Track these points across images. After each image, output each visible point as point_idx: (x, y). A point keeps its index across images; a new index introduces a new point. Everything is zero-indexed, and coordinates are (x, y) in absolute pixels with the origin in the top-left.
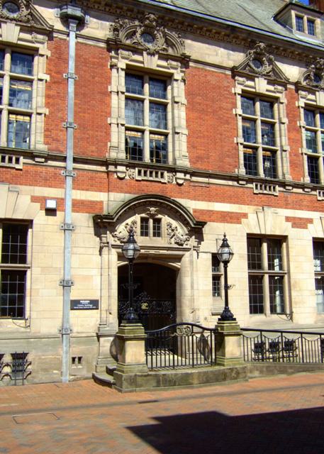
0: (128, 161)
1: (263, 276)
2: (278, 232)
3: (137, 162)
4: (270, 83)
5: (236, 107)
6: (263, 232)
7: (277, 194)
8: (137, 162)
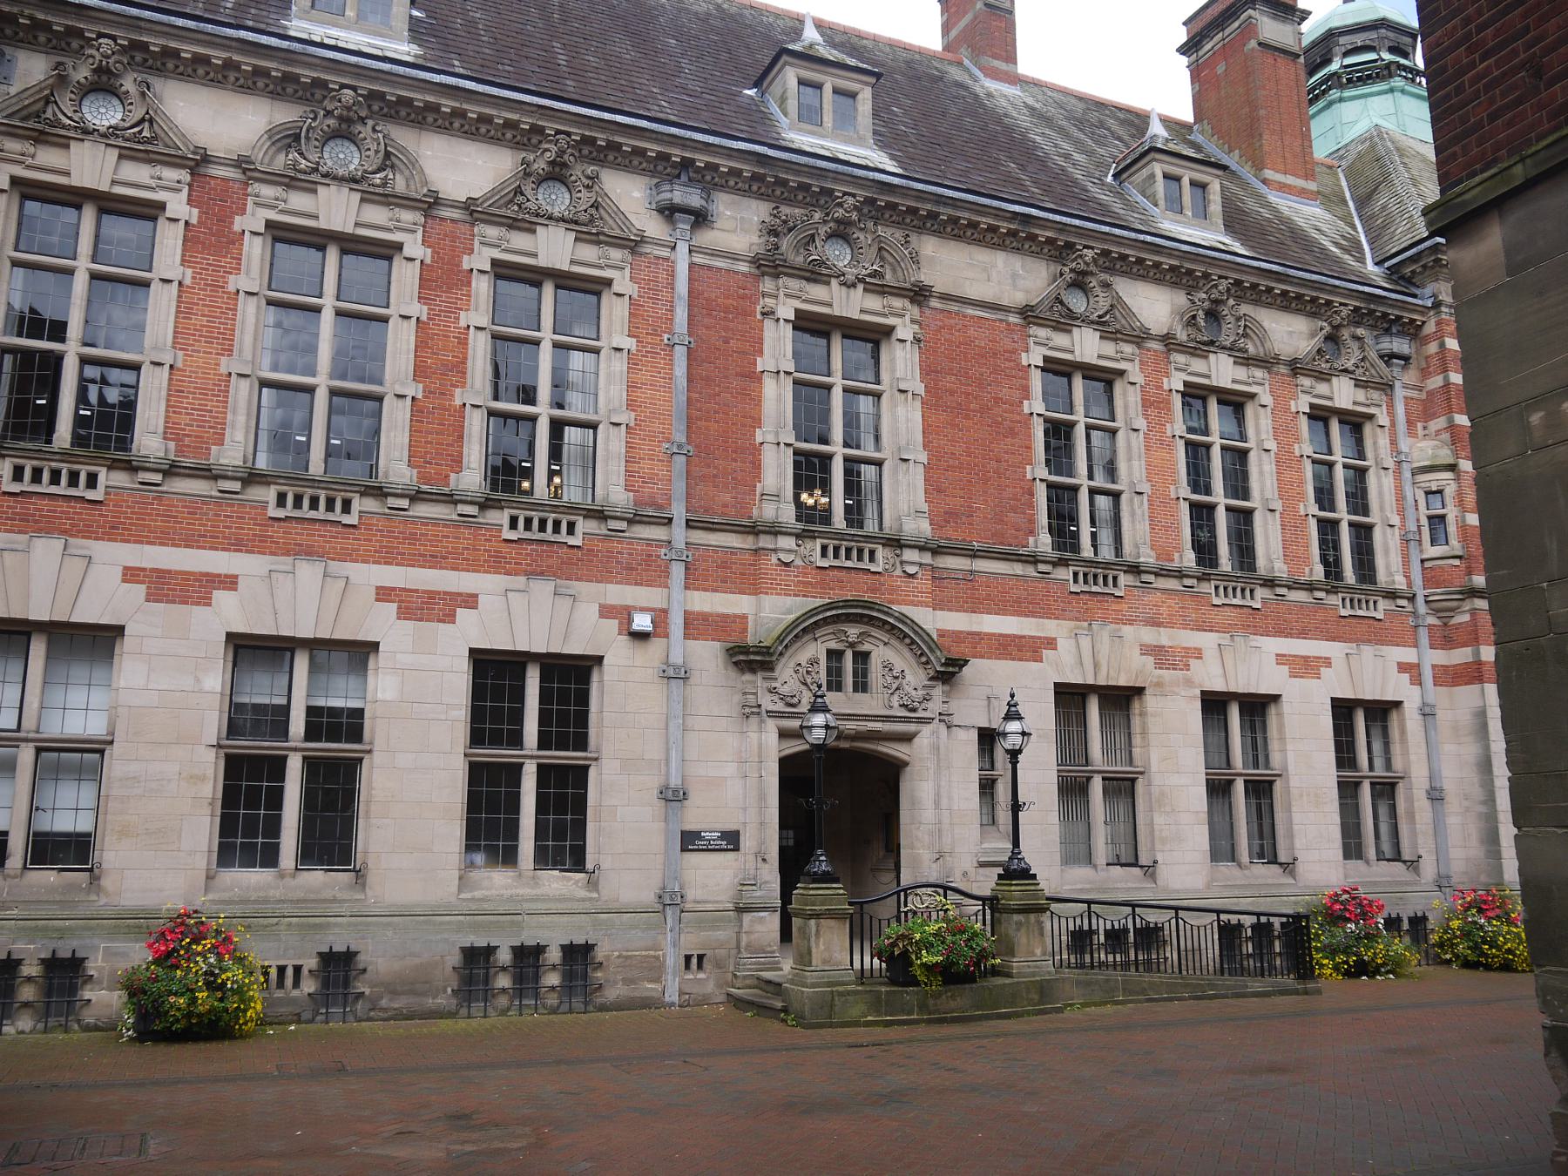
0: (1057, 554)
1: (1230, 783)
2: (1264, 689)
3: (1067, 555)
4: (1358, 384)
5: (1298, 440)
6: (1232, 689)
7: (1258, 606)
8: (1067, 555)
